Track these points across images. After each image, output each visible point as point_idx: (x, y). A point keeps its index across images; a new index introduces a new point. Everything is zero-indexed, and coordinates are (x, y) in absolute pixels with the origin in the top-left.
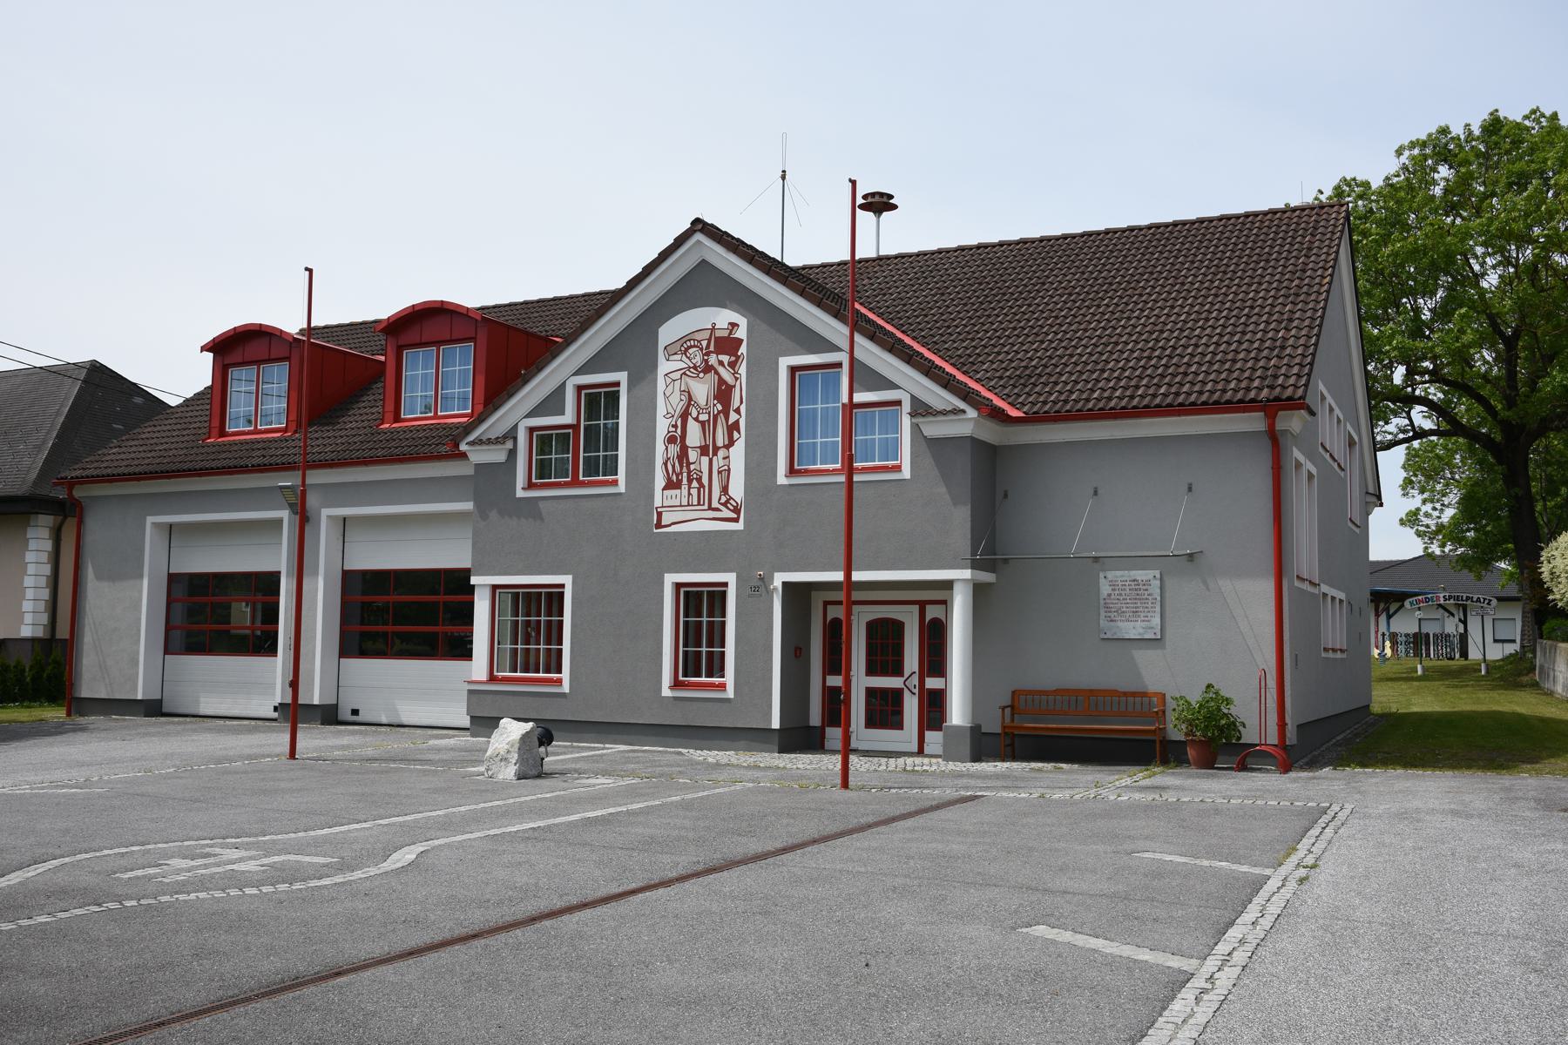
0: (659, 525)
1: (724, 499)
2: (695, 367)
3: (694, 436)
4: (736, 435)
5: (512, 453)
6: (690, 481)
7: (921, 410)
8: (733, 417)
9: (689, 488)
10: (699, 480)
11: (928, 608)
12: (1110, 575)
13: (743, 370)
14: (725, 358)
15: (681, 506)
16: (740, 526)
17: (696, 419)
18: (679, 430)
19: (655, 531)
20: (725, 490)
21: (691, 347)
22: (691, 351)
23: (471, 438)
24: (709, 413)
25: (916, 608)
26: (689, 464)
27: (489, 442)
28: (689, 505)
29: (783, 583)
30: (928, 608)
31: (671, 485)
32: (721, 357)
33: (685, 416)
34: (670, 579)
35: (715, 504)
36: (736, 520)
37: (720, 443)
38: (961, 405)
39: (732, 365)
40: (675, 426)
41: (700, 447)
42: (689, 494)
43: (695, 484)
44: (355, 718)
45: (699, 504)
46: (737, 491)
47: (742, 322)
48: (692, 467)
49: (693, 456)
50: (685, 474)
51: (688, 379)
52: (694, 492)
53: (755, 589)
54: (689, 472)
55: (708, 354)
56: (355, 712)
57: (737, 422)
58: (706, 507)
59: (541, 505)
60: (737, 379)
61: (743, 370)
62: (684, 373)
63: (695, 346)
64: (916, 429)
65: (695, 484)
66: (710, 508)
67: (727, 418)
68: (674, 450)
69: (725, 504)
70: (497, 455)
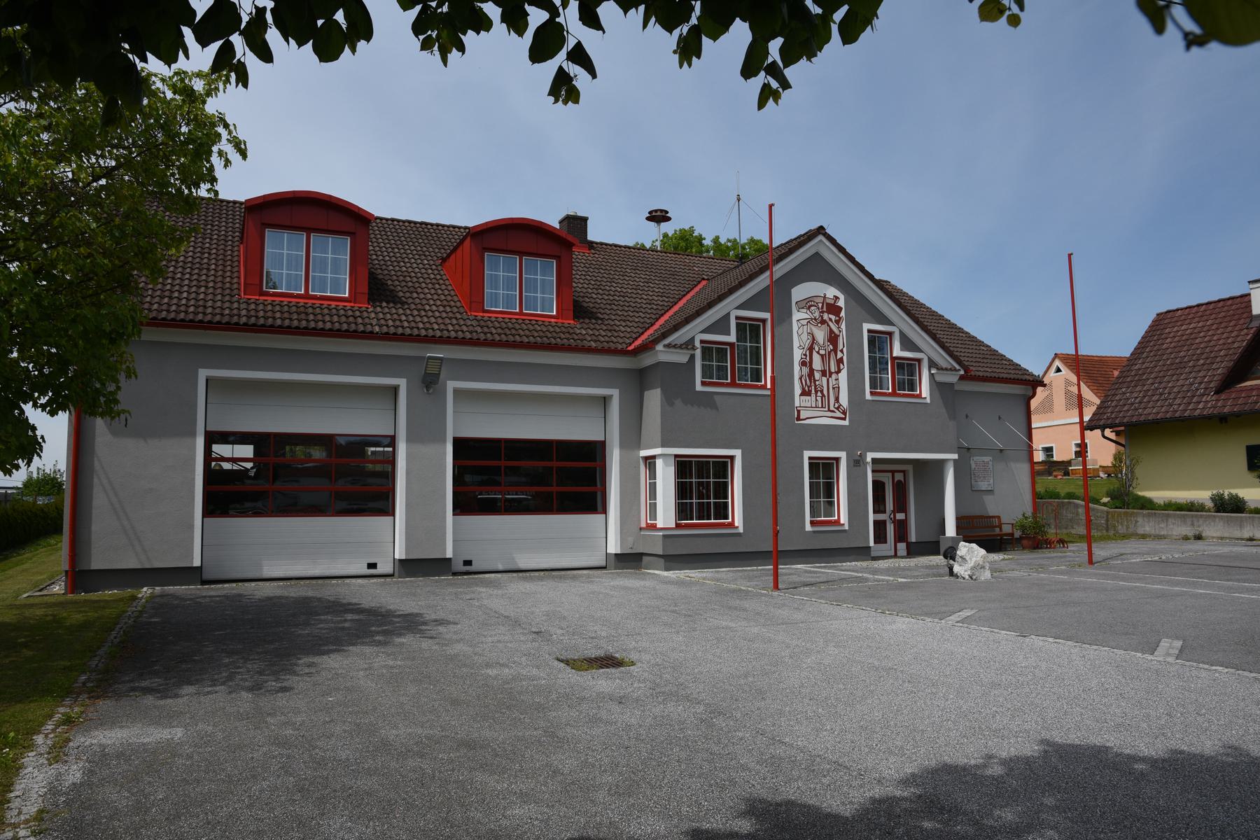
0: (798, 419)
1: (837, 405)
2: (815, 319)
3: (817, 364)
4: (842, 366)
5: (692, 357)
6: (816, 392)
7: (932, 364)
8: (840, 355)
9: (816, 396)
10: (822, 392)
11: (896, 474)
12: (975, 458)
13: (843, 326)
14: (833, 317)
15: (812, 407)
16: (846, 423)
17: (818, 352)
18: (808, 358)
19: (796, 422)
20: (837, 399)
21: (812, 306)
22: (813, 308)
23: (667, 341)
24: (825, 350)
25: (890, 474)
26: (815, 381)
27: (675, 346)
28: (816, 407)
29: (872, 459)
30: (896, 474)
31: (804, 393)
32: (831, 316)
33: (811, 349)
34: (807, 454)
35: (832, 408)
36: (844, 419)
37: (833, 370)
38: (958, 367)
39: (837, 322)
40: (805, 355)
41: (821, 371)
42: (816, 400)
43: (819, 394)
44: (468, 568)
45: (822, 407)
46: (844, 400)
47: (842, 297)
48: (817, 383)
49: (817, 376)
50: (813, 387)
51: (811, 326)
52: (819, 399)
53: (856, 463)
54: (816, 386)
55: (823, 312)
56: (468, 563)
57: (842, 358)
58: (827, 409)
59: (717, 398)
60: (840, 331)
61: (843, 326)
62: (809, 322)
63: (814, 306)
64: (932, 376)
65: (819, 394)
66: (829, 410)
67: (836, 356)
68: (805, 370)
69: (837, 409)
70: (681, 357)
